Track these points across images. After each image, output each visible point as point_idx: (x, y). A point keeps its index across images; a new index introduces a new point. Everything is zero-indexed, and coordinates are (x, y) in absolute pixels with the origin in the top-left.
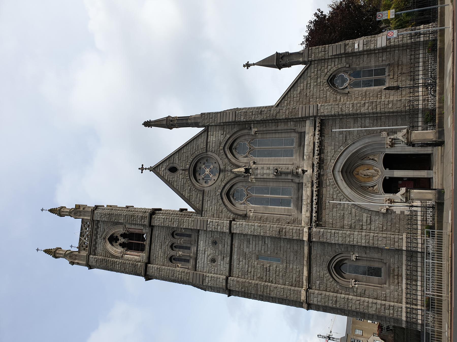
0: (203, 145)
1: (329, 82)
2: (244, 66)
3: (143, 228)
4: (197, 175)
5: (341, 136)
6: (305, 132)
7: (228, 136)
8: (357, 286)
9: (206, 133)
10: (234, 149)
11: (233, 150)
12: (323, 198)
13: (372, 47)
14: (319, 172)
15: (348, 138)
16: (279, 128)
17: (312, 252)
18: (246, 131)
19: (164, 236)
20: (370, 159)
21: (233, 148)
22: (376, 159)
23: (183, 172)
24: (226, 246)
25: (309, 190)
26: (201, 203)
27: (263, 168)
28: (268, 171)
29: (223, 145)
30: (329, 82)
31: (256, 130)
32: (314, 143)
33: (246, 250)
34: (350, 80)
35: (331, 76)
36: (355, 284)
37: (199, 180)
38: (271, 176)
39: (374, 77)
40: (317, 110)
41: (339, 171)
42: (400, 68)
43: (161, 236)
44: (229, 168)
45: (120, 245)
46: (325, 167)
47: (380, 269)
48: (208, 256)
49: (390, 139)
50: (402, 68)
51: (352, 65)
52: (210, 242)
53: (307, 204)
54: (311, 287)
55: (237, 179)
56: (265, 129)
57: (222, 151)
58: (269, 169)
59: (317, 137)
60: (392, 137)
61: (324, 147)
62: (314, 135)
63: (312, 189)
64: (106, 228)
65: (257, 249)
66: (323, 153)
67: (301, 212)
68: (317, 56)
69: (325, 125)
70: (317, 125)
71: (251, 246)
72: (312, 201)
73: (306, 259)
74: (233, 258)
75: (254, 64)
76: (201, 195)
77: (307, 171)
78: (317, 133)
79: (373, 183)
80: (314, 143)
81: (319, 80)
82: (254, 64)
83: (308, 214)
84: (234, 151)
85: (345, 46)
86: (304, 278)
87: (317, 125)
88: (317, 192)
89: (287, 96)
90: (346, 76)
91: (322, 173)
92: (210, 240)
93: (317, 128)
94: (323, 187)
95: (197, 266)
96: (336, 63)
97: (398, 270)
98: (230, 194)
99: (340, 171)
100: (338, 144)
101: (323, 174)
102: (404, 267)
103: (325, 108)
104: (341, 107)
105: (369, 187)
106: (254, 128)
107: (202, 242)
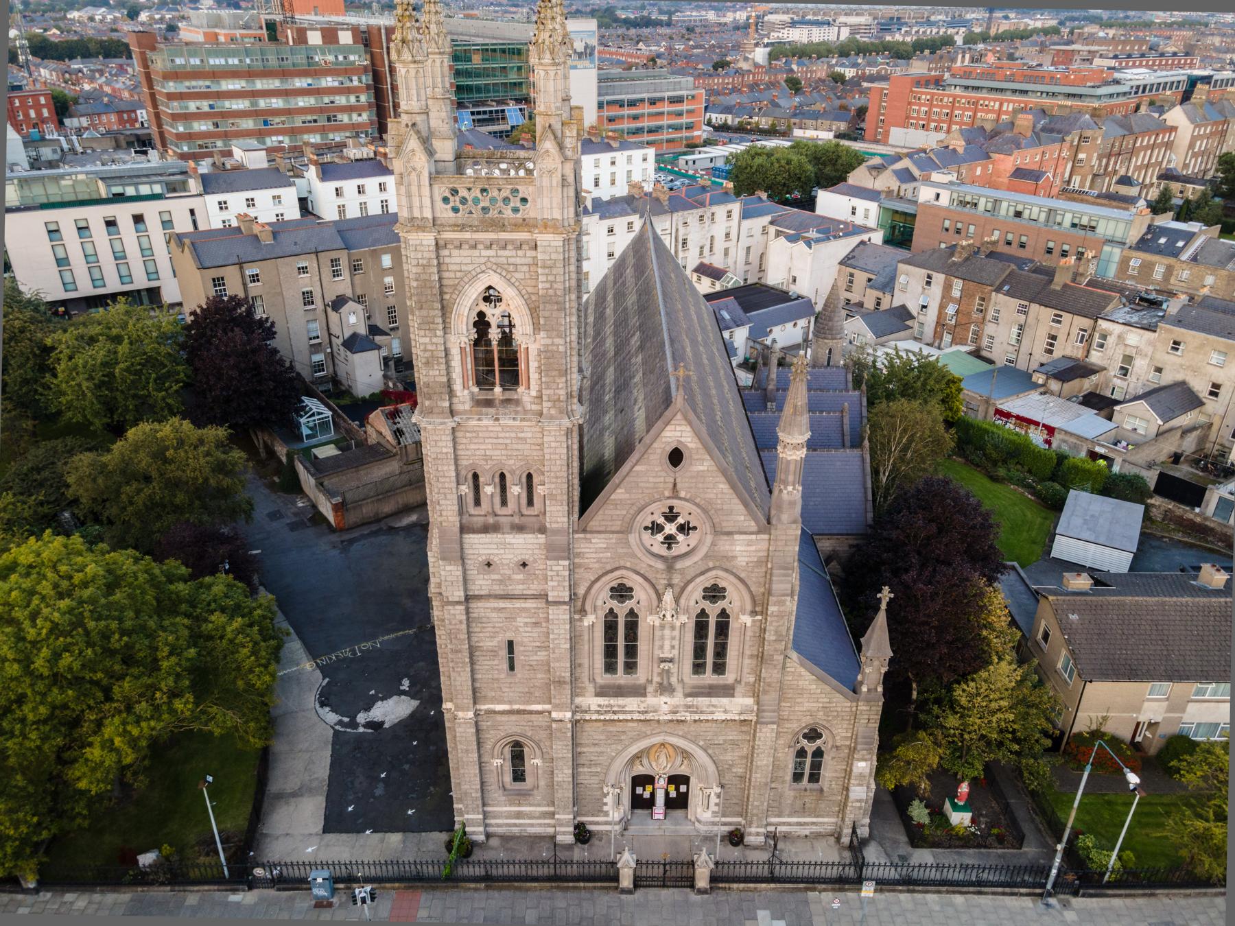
0: (727, 526)
3: (534, 393)
6: (733, 696)
7: (743, 575)
13: (852, 781)
16: (747, 661)
18: (749, 607)
23: (671, 486)
24: (521, 587)
25: (635, 708)
26: (602, 529)
29: (728, 565)
31: (749, 624)
33: (521, 621)
38: (657, 652)
39: (807, 771)
43: (520, 447)
44: (676, 580)
45: (481, 315)
47: (524, 780)
53: (611, 706)
55: (654, 596)
56: (747, 638)
58: (673, 647)
64: (518, 275)
67: (597, 695)
72: (615, 713)
73: (522, 707)
76: (618, 529)
83: (594, 707)
86: (492, 707)
106: (754, 621)
107: (521, 541)
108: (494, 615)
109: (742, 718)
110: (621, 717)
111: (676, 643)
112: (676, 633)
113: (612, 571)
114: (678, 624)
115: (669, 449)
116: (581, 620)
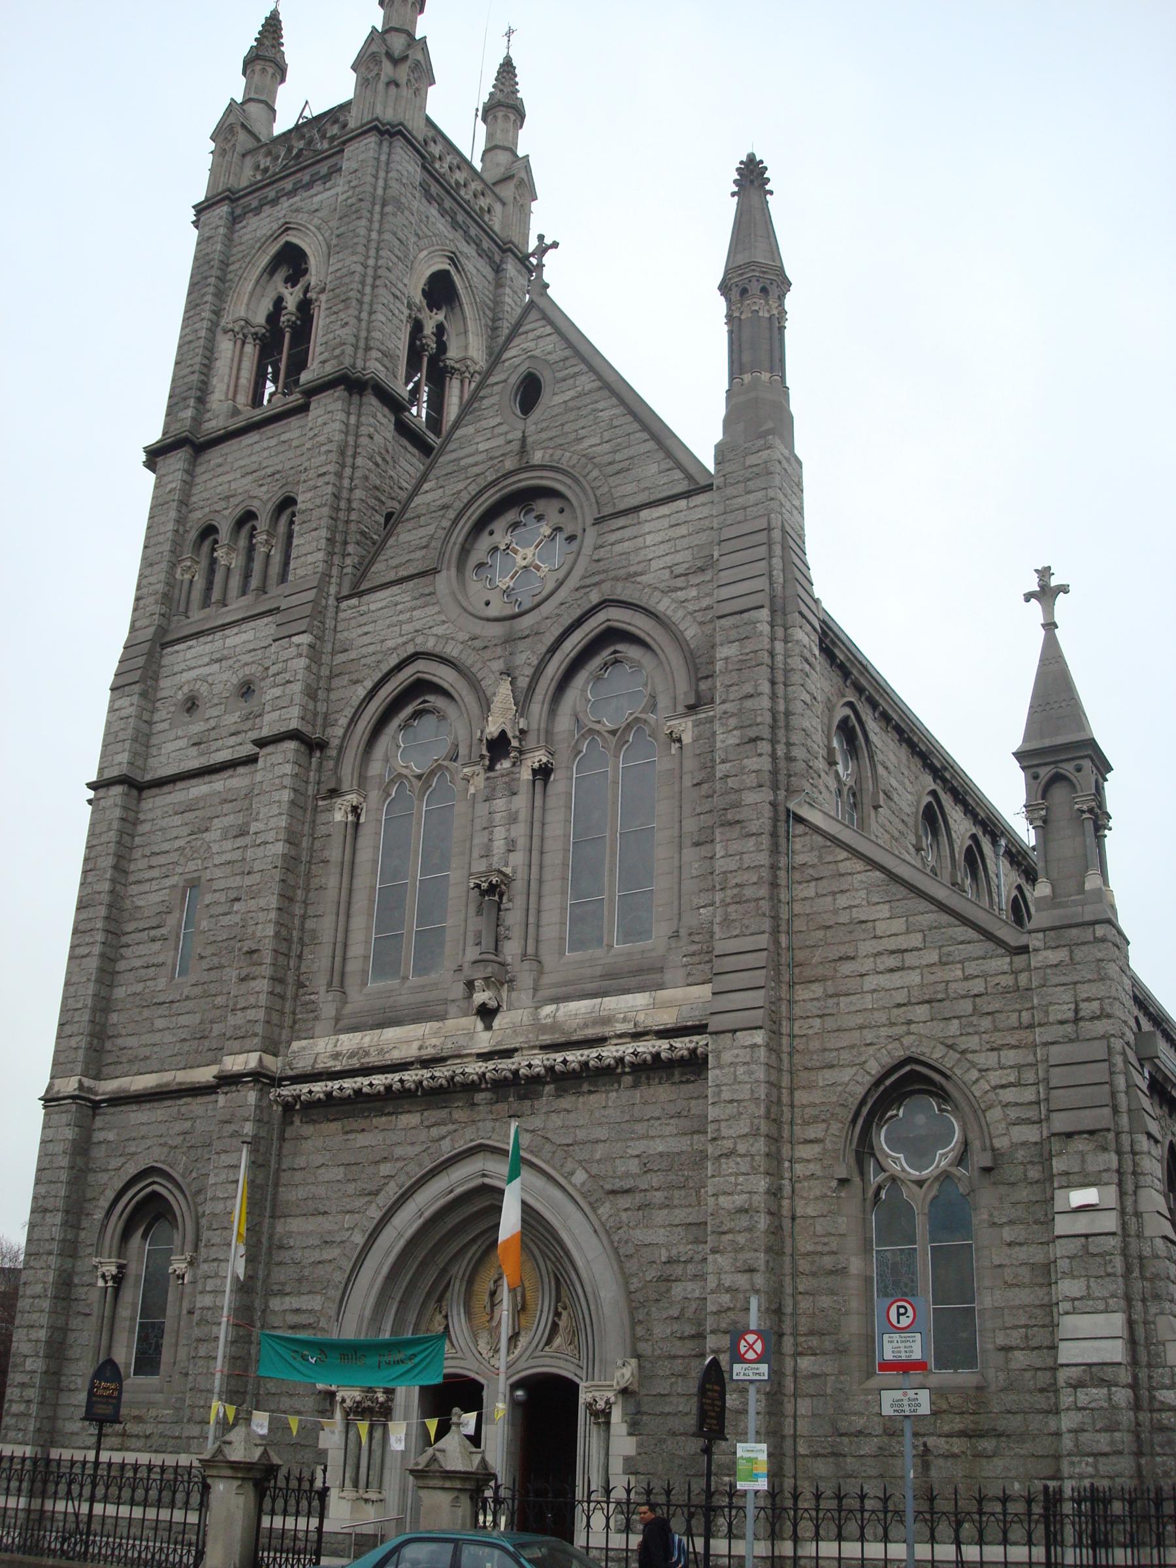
1: (907, 1068)
2: (1044, 573)
4: (511, 516)
5: (634, 1166)
8: (101, 1283)
9: (682, 487)
10: (616, 652)
11: (611, 649)
12: (384, 1119)
14: (483, 1086)
15: (624, 1202)
17: (200, 1100)
19: (279, 467)
20: (558, 1314)
21: (619, 647)
22: (558, 1341)
23: (515, 446)
27: (513, 819)
28: (499, 846)
29: (623, 592)
30: (907, 1068)
31: (687, 739)
32: (601, 1041)
34: (920, 1183)
35: (937, 1077)
36: (104, 1276)
37: (491, 533)
40: (735, 1031)
41: (484, 1175)
42: (957, 1445)
46: (502, 1107)
48: (203, 679)
49: (607, 1402)
50: (954, 1456)
51: (994, 1184)
52: (247, 670)
54: (101, 1111)
57: (595, 598)
58: (511, 847)
59: (626, 1049)
60: (616, 1416)
61: (590, 1092)
62: (637, 1036)
63: (412, 1063)
65: (218, 873)
66: (560, 1093)
68: (1056, 980)
69: (688, 1082)
70: (678, 1043)
71: (228, 845)
74: (193, 782)
75: (1050, 626)
77: (488, 1027)
78: (646, 1047)
79: (458, 1332)
80: (601, 1041)
81: (922, 1012)
82: (1050, 626)
84: (605, 655)
85: (1091, 1133)
87: (683, 1044)
88: (397, 1086)
89: (844, 855)
90: (943, 1158)
91: (480, 1097)
92: (253, 668)
93: (664, 1044)
94: (426, 1114)
95: (176, 648)
96: (1008, 1095)
97: (137, 1436)
98: (427, 698)
99: (487, 1180)
100: (598, 1157)
101: (474, 1104)
102: (144, 1458)
103: (741, 1070)
104: (742, 1148)
105: (446, 1317)
108: (177, 820)
109: (683, 1044)
110: (379, 1080)
111: (519, 831)
112: (521, 802)
113: (399, 667)
114: (526, 774)
115: (514, 379)
116: (330, 810)
